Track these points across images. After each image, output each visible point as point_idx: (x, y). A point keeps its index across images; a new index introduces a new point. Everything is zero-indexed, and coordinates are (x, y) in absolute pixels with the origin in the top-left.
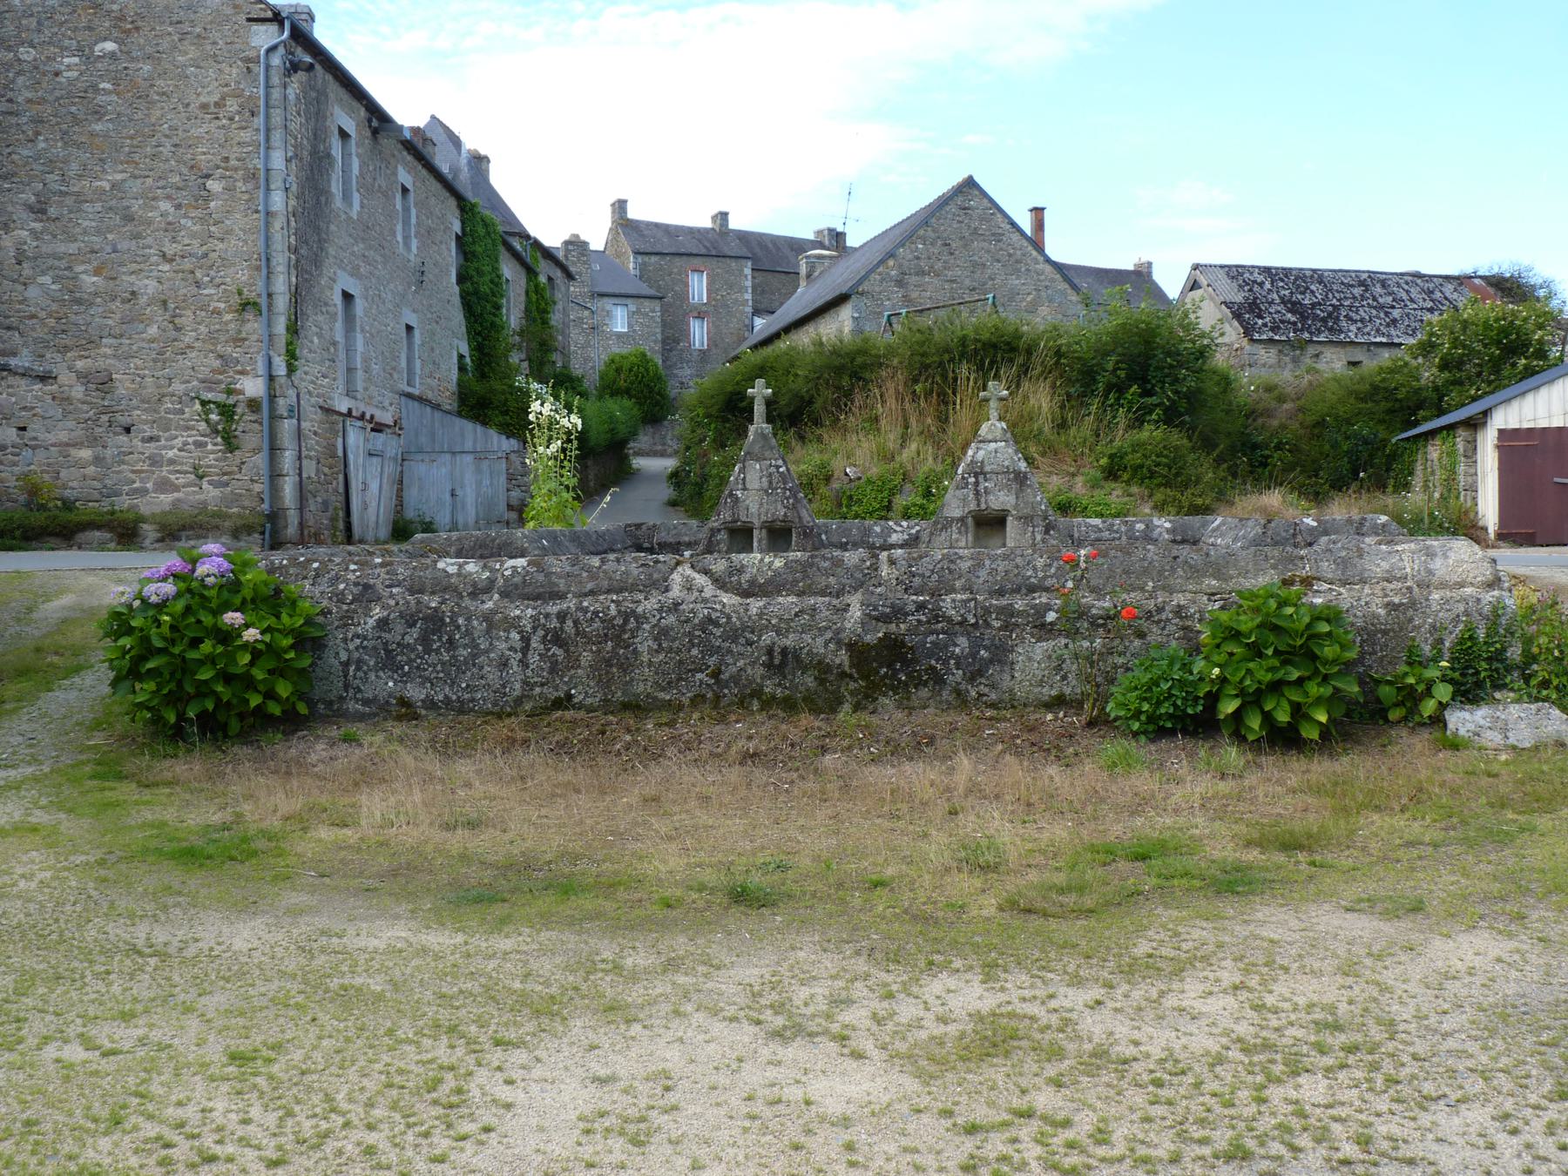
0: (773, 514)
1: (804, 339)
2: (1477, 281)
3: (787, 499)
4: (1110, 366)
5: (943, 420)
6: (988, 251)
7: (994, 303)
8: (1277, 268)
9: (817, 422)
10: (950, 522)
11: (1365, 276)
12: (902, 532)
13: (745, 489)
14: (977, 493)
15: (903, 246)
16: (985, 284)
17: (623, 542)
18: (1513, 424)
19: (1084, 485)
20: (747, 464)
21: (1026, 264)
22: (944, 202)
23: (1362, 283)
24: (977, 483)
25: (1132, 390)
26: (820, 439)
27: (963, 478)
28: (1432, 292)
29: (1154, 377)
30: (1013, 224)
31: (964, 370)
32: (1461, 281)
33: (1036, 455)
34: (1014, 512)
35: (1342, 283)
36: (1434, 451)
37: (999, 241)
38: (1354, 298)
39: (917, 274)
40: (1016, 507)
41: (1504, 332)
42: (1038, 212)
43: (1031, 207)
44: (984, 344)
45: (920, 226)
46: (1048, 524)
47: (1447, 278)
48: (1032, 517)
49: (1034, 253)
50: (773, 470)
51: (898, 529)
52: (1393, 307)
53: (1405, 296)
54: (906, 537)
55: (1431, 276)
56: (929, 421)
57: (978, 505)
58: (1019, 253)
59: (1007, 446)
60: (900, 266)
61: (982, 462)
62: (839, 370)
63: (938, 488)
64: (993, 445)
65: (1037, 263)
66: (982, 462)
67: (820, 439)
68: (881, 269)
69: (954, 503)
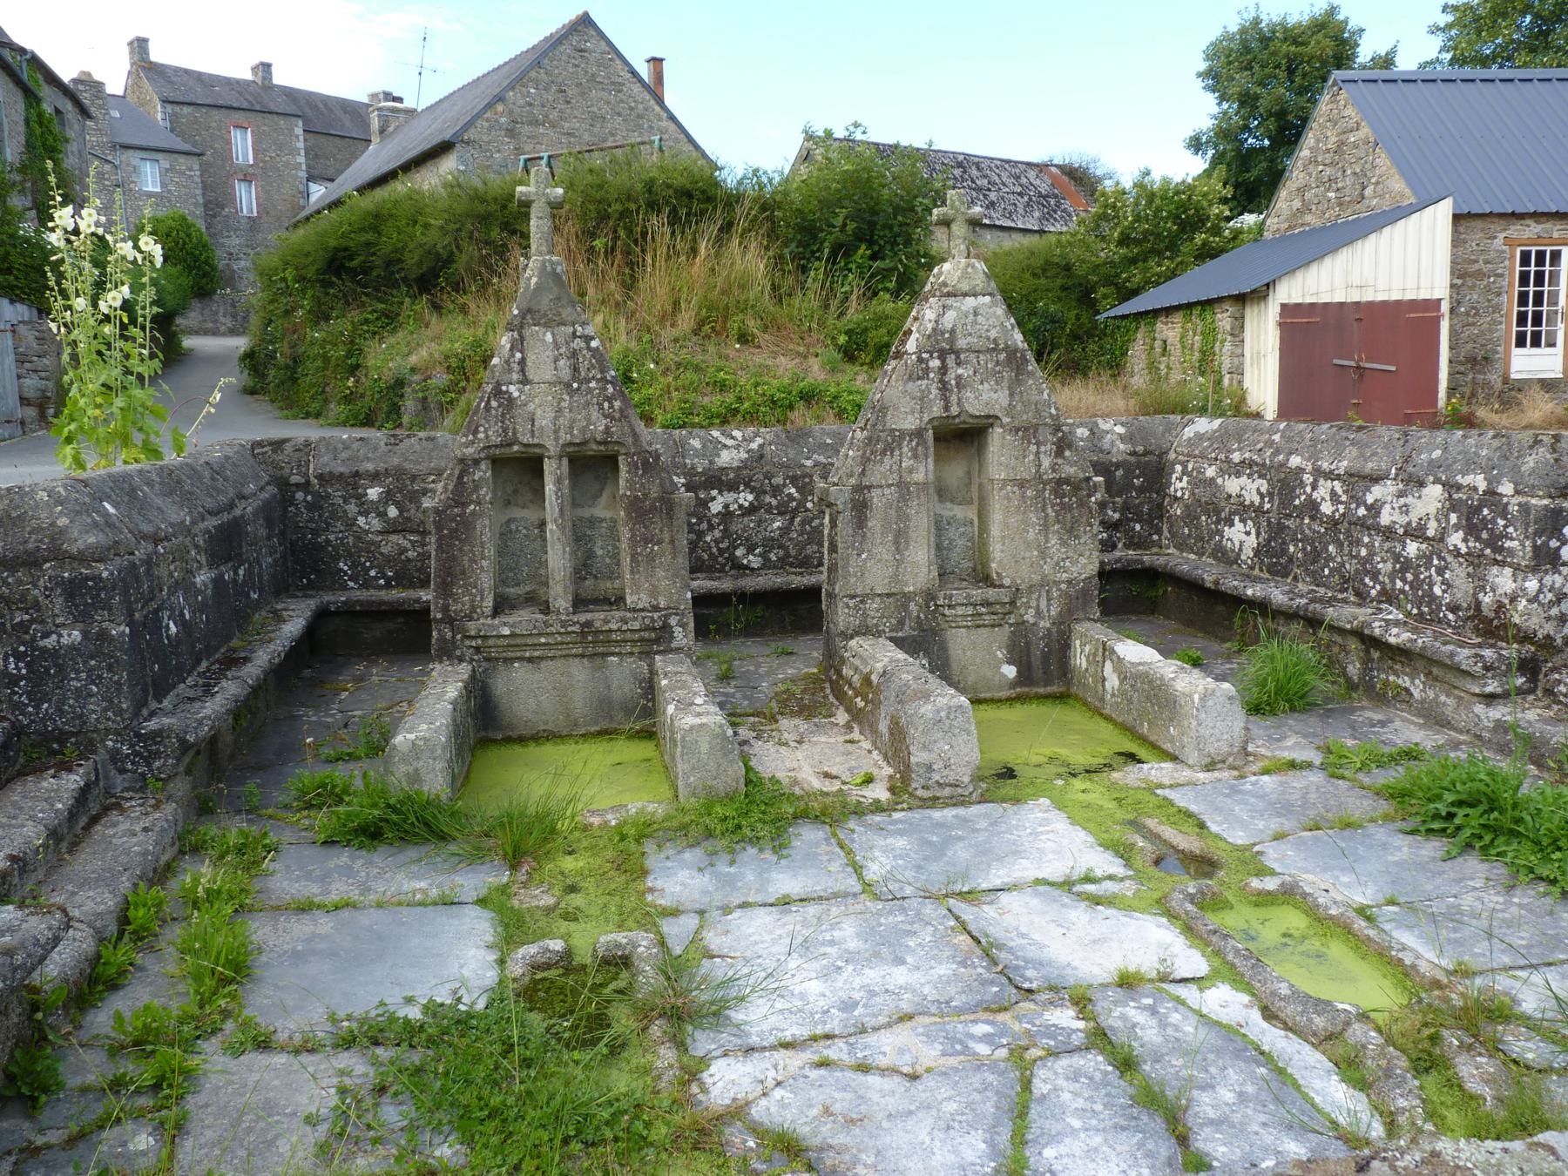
0: (584, 430)
1: (430, 180)
2: (1053, 169)
3: (609, 400)
4: (839, 221)
5: (630, 285)
6: (608, 103)
7: (661, 149)
8: (884, 145)
9: (458, 287)
10: (899, 437)
11: (961, 158)
12: (737, 447)
13: (525, 381)
14: (944, 387)
15: (513, 88)
16: (605, 141)
17: (257, 477)
18: (1296, 298)
19: (823, 367)
20: (527, 332)
21: (648, 120)
22: (555, 43)
23: (960, 165)
24: (943, 370)
25: (860, 252)
26: (464, 310)
27: (920, 360)
28: (1019, 177)
29: (881, 237)
30: (634, 73)
31: (658, 224)
32: (1042, 168)
33: (755, 330)
34: (1006, 420)
35: (943, 163)
36: (1169, 331)
37: (620, 91)
38: (955, 178)
39: (530, 123)
40: (1010, 410)
41: (1183, 207)
42: (656, 62)
43: (649, 56)
44: (676, 191)
45: (531, 67)
46: (1061, 440)
47: (1029, 164)
48: (1036, 427)
49: (657, 108)
50: (578, 344)
51: (729, 442)
52: (989, 190)
53: (996, 178)
54: (744, 455)
55: (1016, 162)
56: (613, 286)
57: (947, 408)
58: (641, 107)
59: (994, 304)
60: (511, 112)
61: (953, 331)
62: (485, 219)
63: (639, 372)
64: (970, 302)
65: (660, 120)
66: (953, 331)
67: (464, 310)
68: (488, 115)
69: (906, 404)
